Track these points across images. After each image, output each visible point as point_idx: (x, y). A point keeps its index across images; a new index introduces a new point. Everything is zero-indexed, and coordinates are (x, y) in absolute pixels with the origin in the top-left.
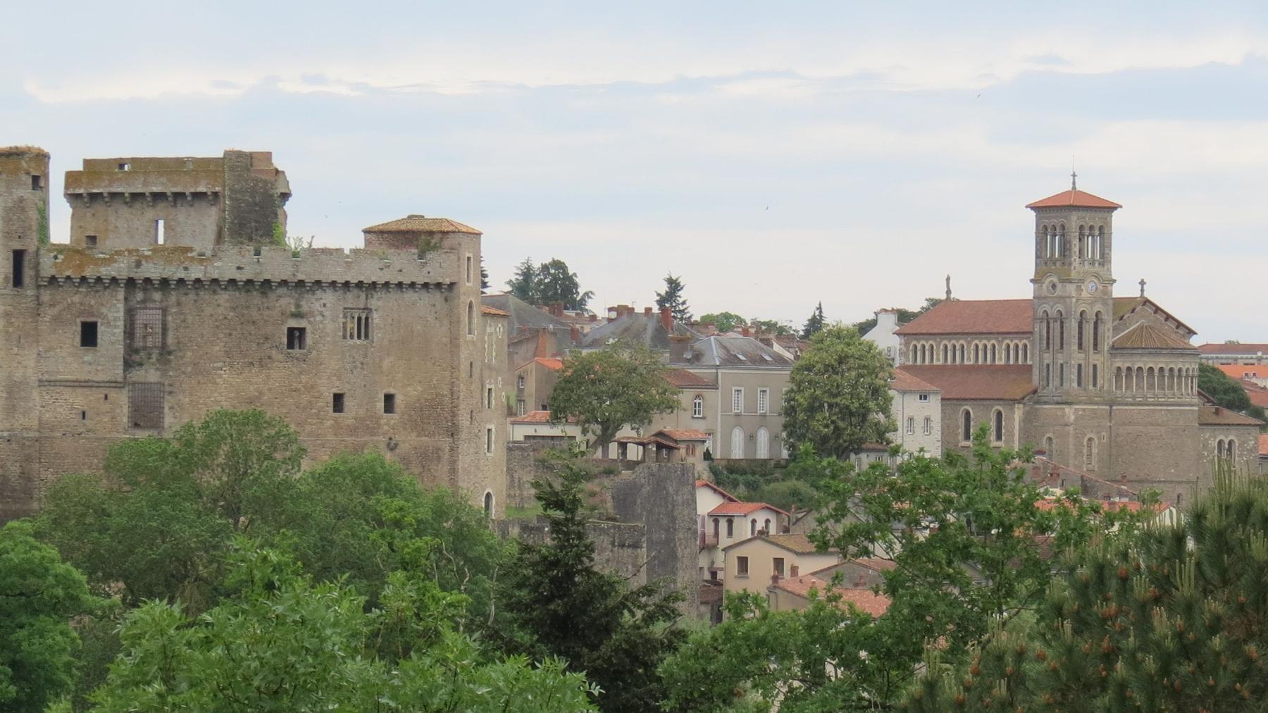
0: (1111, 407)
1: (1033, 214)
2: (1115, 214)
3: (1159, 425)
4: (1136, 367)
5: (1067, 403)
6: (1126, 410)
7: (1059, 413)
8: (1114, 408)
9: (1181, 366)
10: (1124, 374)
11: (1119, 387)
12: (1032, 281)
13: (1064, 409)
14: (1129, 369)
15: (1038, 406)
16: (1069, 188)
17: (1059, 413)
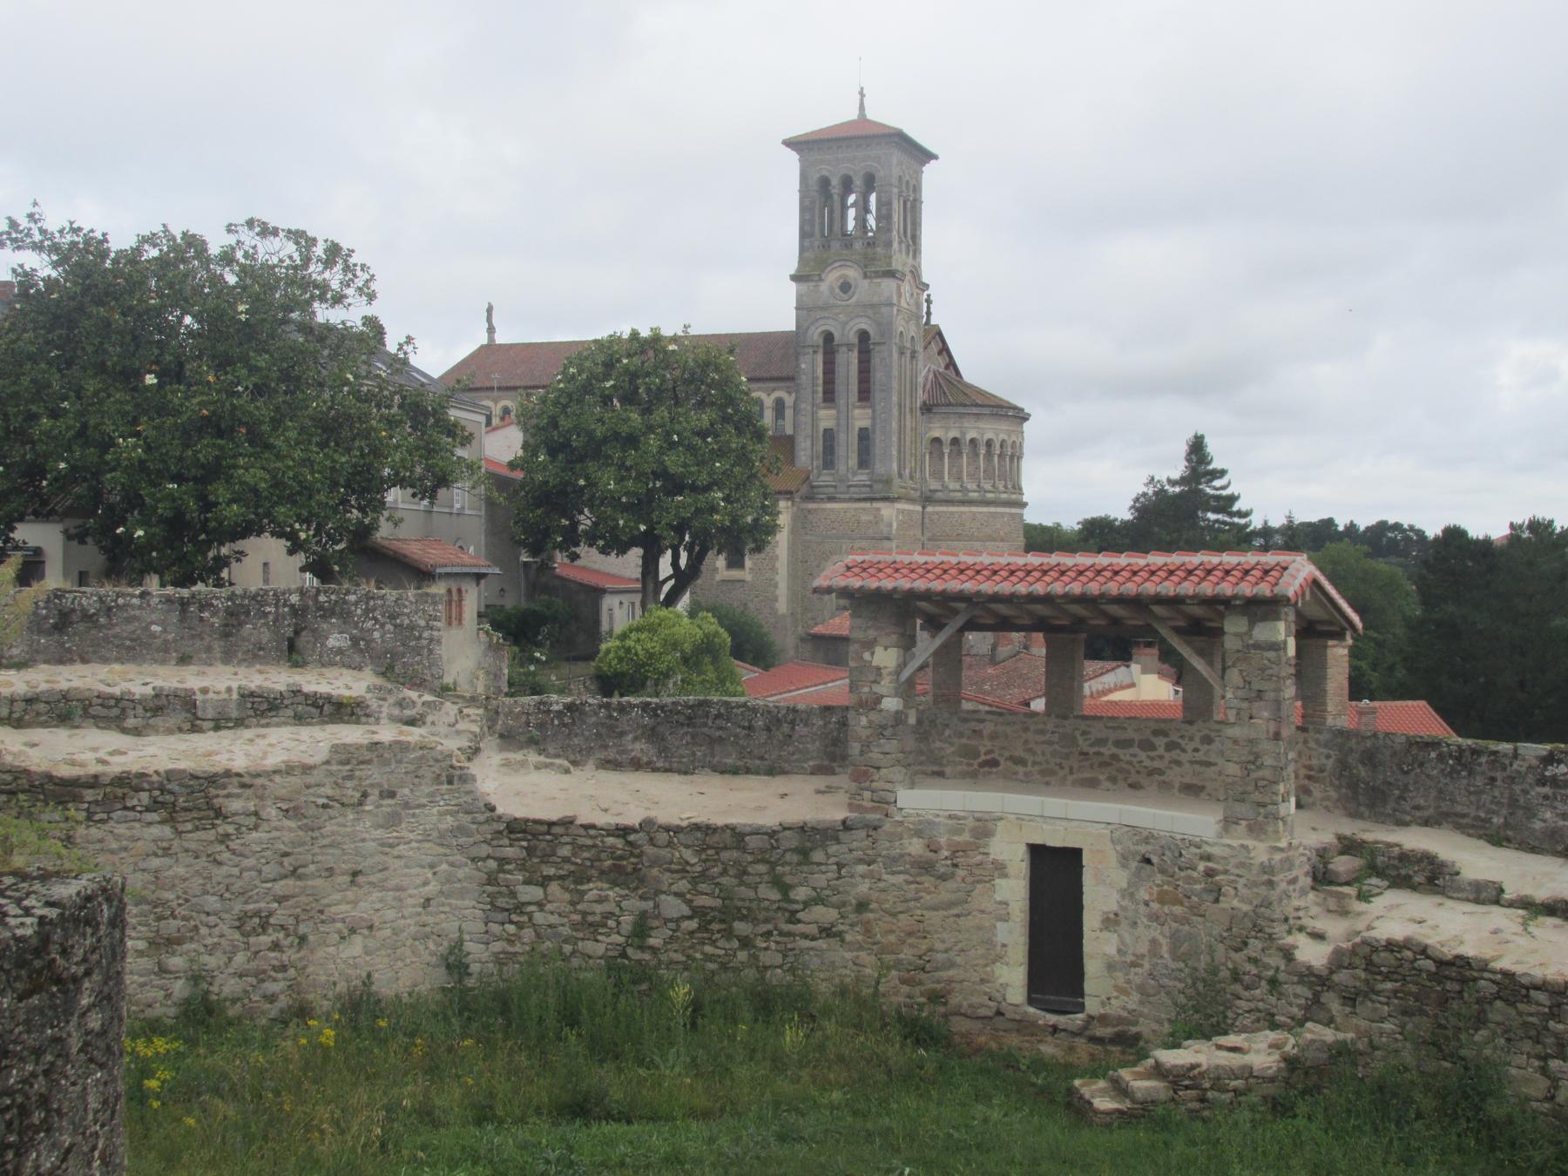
0: (924, 508)
1: (793, 158)
2: (929, 170)
3: (1002, 540)
4: (968, 437)
5: (885, 499)
6: (952, 513)
7: (864, 518)
8: (929, 509)
9: (1006, 437)
10: (946, 451)
11: (937, 475)
12: (794, 278)
13: (879, 509)
14: (955, 441)
15: (811, 506)
16: (853, 115)
17: (864, 518)
